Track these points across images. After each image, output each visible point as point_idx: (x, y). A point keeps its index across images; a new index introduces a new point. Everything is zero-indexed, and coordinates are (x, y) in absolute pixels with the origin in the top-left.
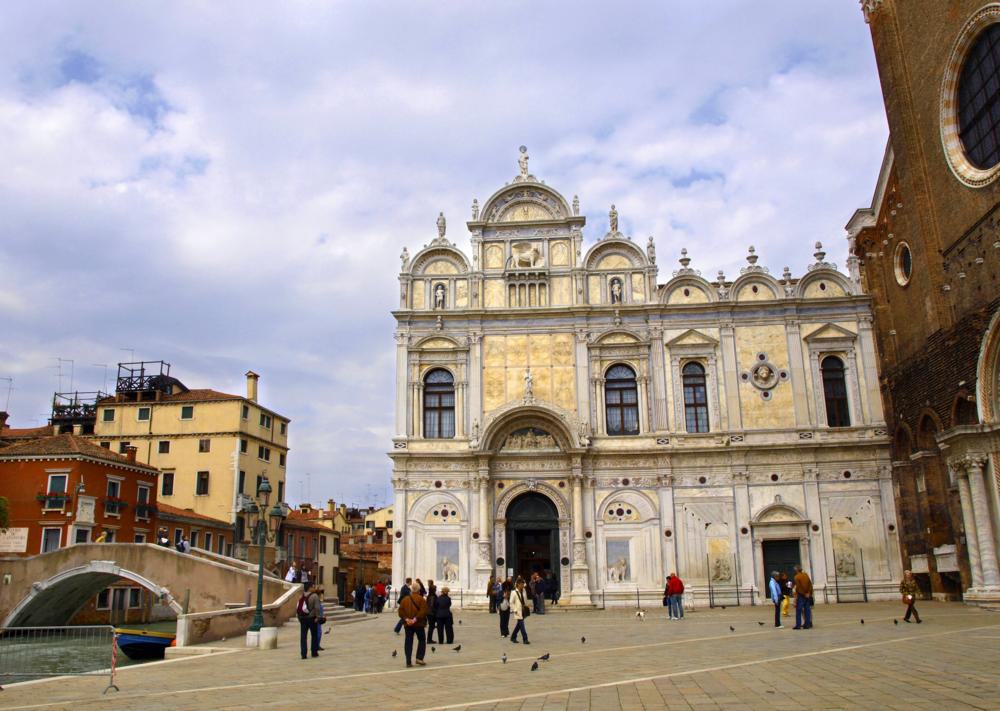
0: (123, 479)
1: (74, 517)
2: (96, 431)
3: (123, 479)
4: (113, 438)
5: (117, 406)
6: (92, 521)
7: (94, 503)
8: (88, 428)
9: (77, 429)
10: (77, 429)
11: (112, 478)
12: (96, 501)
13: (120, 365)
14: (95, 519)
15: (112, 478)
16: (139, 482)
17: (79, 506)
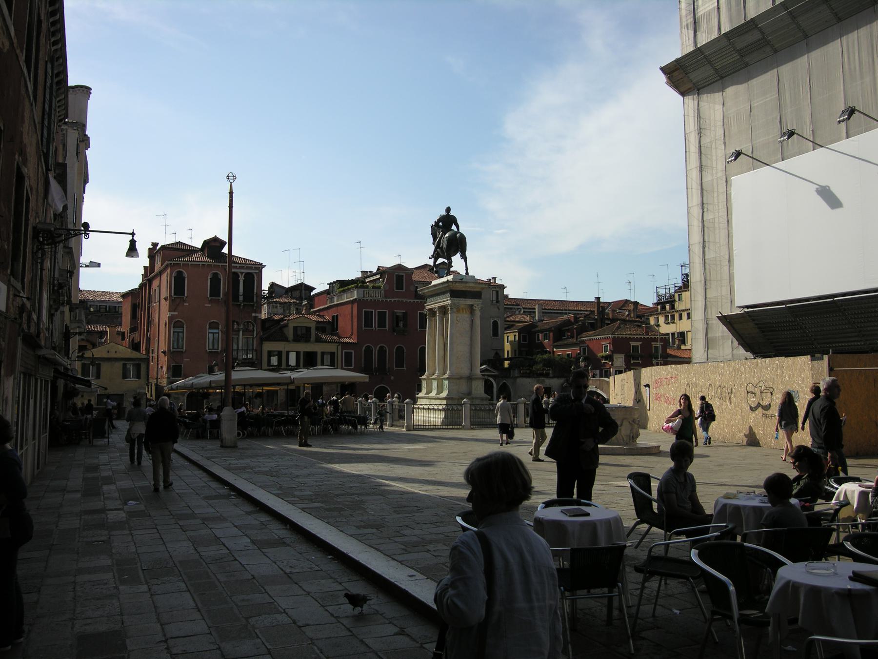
0: (641, 343)
1: (612, 364)
2: (675, 307)
3: (641, 343)
4: (683, 311)
5: (683, 291)
6: (624, 366)
7: (623, 357)
8: (673, 307)
9: (668, 306)
10: (668, 306)
11: (633, 344)
12: (625, 356)
13: (682, 266)
14: (625, 366)
15: (633, 344)
16: (652, 343)
17: (614, 359)
